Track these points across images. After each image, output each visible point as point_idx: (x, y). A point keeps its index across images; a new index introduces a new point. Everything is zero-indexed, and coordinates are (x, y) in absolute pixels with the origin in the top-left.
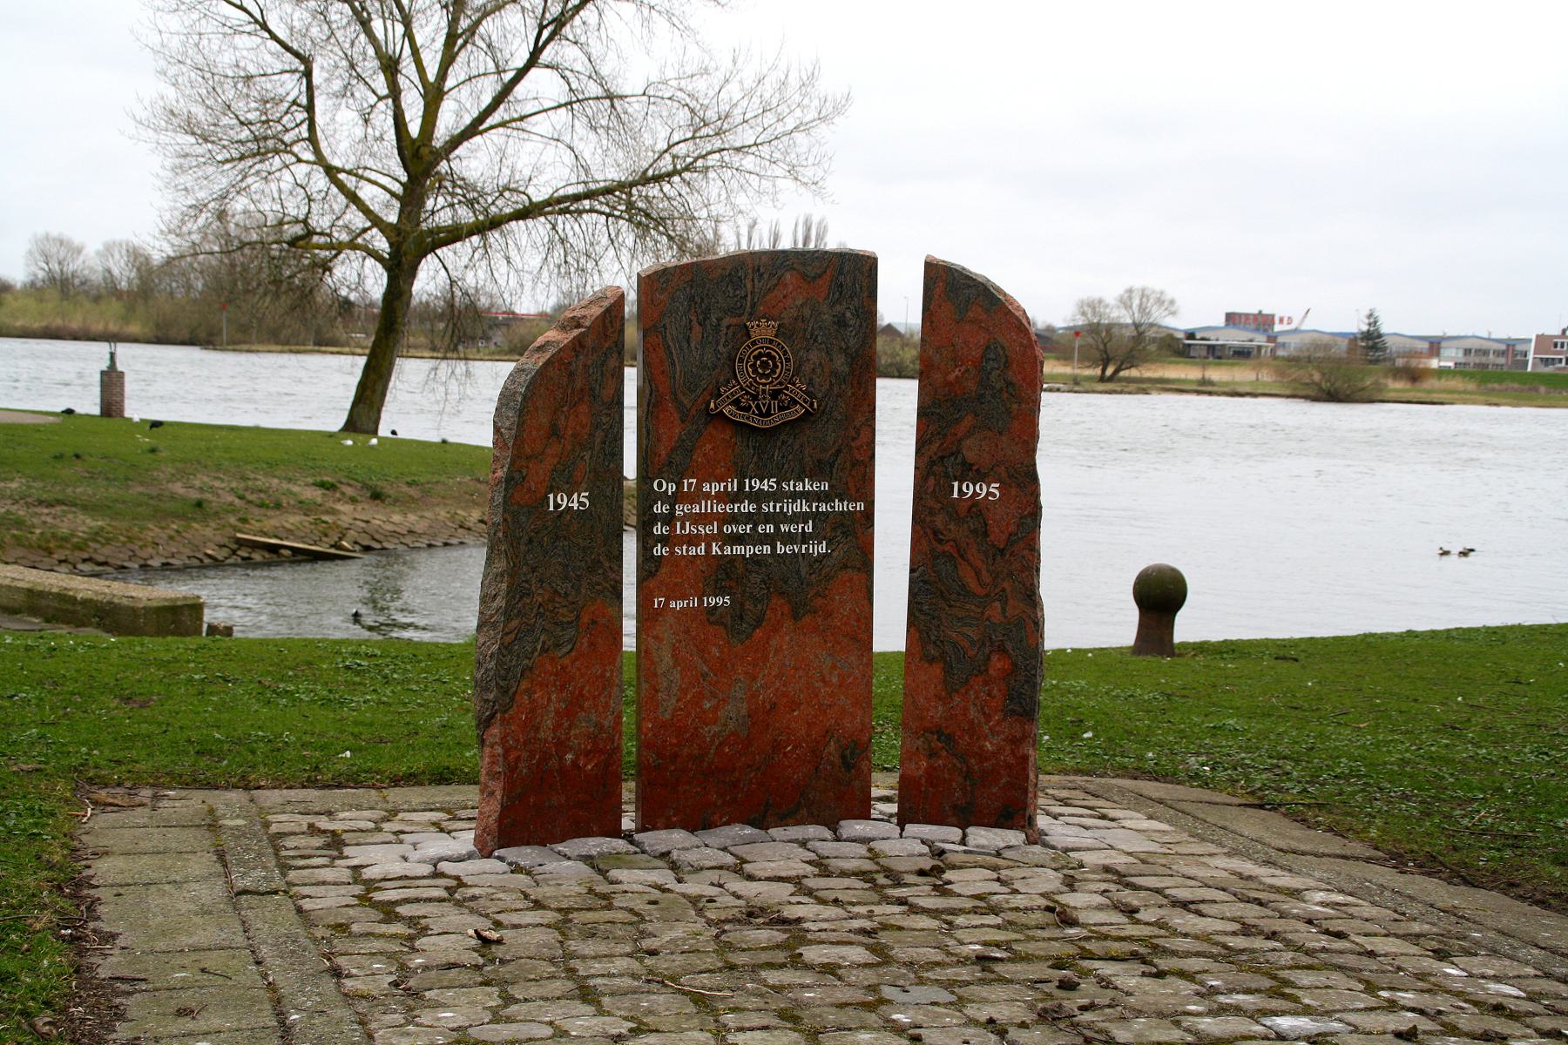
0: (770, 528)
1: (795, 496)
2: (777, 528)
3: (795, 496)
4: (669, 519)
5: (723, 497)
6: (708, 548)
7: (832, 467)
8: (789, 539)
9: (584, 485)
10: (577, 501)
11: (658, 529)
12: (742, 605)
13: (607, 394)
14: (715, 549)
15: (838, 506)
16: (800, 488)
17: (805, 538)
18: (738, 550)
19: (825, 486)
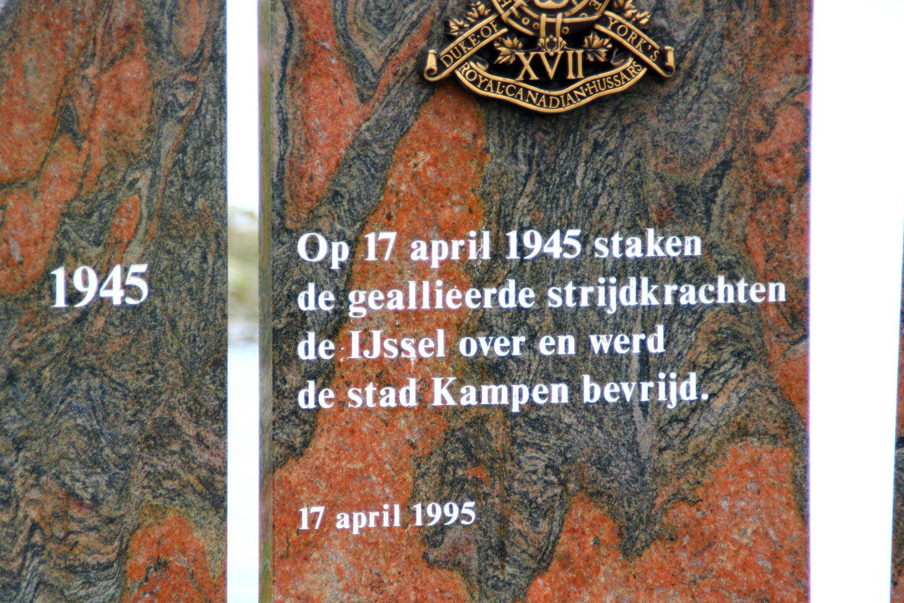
0: (567, 345)
1: (623, 270)
2: (583, 345)
3: (623, 270)
5: (458, 274)
6: (425, 388)
7: (710, 200)
8: (611, 367)
9: (136, 249)
10: (122, 284)
11: (310, 348)
12: (503, 521)
13: (187, 37)
14: (440, 394)
15: (725, 291)
16: (634, 250)
17: (647, 367)
18: (494, 394)
19: (694, 246)
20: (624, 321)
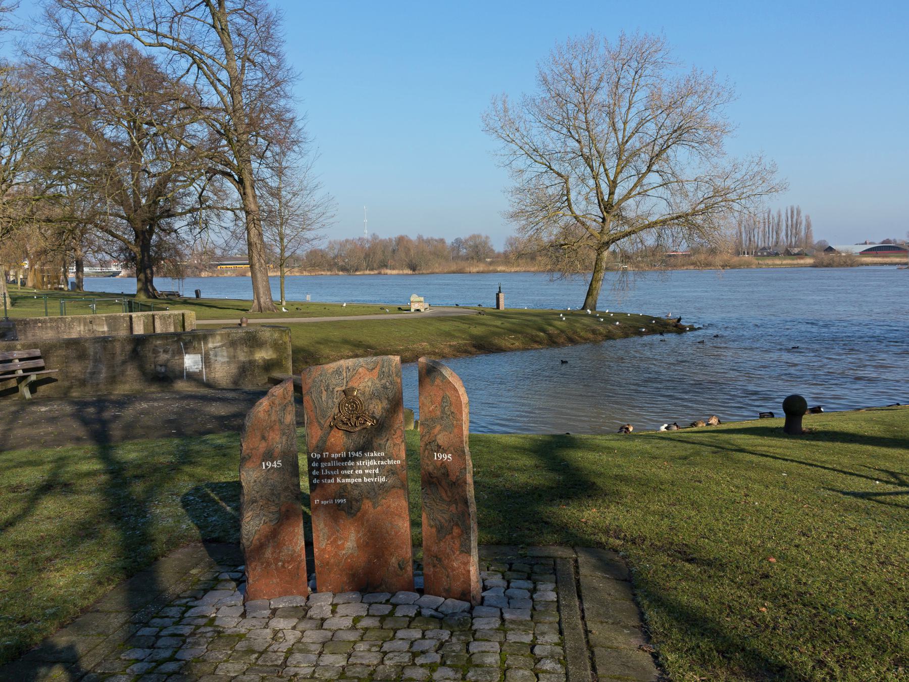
0: (361, 472)
2: (364, 472)
4: (319, 469)
6: (335, 480)
8: (369, 476)
11: (314, 473)
14: (338, 480)
16: (372, 455)
17: (376, 475)
20: (371, 467)
